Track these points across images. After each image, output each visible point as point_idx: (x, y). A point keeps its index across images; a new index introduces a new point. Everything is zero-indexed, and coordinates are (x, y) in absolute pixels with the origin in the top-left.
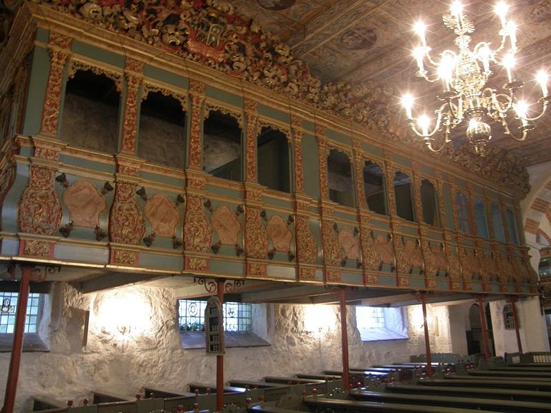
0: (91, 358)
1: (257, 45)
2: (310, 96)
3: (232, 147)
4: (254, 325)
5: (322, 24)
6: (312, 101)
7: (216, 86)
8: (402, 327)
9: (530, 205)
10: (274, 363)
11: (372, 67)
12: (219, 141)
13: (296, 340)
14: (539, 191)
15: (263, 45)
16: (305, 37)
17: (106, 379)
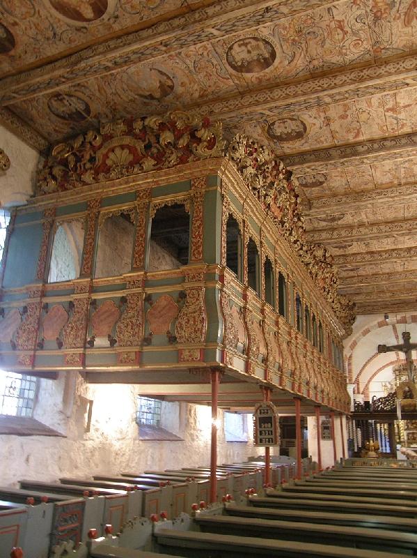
0: (89, 444)
1: (294, 211)
2: (301, 252)
3: (172, 260)
4: (163, 420)
5: (330, 205)
6: (301, 255)
7: (268, 235)
8: (242, 431)
9: (350, 344)
10: (184, 456)
11: (324, 235)
12: (166, 255)
13: (195, 437)
14: (358, 335)
15: (296, 212)
16: (310, 209)
17: (97, 465)
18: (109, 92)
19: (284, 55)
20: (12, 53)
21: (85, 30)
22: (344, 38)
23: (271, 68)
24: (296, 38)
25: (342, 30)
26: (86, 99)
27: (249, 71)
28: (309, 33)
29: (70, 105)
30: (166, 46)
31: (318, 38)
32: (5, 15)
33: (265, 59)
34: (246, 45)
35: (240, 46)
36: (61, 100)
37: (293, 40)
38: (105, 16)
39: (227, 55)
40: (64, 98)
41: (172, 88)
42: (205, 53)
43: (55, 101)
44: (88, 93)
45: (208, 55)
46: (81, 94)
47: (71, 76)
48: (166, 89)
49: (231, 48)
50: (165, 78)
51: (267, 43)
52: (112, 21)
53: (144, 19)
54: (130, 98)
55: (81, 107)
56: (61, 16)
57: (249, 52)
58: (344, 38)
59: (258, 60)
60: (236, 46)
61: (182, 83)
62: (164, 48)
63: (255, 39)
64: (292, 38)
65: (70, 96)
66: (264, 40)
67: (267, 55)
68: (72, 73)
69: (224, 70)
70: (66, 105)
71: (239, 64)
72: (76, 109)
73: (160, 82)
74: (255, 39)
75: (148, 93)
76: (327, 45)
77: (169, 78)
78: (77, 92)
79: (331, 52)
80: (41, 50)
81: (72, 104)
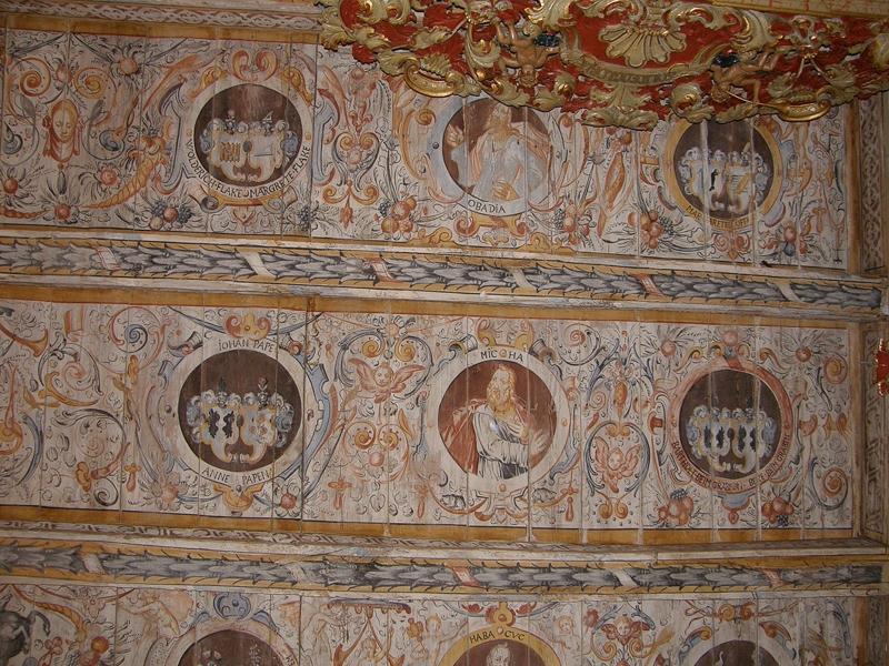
18: (602, 171)
19: (181, 113)
20: (722, 365)
21: (538, 348)
22: (55, 109)
23: (219, 87)
24: (143, 144)
25: (52, 130)
26: (666, 174)
27: (270, 95)
28: (115, 149)
29: (713, 175)
30: (371, 271)
31: (103, 127)
32: (658, 448)
33: (223, 116)
34: (247, 169)
35: (258, 171)
36: (724, 199)
37: (151, 143)
38: (475, 359)
39: (292, 159)
40: (714, 199)
41: (457, 120)
42: (336, 180)
43: (738, 203)
44: (650, 191)
45: (332, 173)
46: (667, 194)
47: (623, 285)
48: (470, 123)
49: (278, 172)
50: (454, 155)
51: (203, 157)
52: (470, 343)
53: (406, 317)
54: (565, 131)
55: (699, 161)
56: (559, 399)
57: (248, 147)
58: (55, 109)
59: (239, 118)
60: (267, 173)
61: (427, 123)
62: (379, 267)
63: (222, 177)
64: (151, 150)
65: (695, 201)
66: (206, 165)
67: (216, 123)
68: (615, 290)
69: (320, 120)
70: (727, 179)
71: (280, 124)
72: (711, 155)
73: (471, 148)
74: (222, 177)
75: (520, 126)
76: (91, 103)
77: (447, 149)
78: (673, 201)
79: (87, 83)
80: (659, 344)
81: (707, 176)
